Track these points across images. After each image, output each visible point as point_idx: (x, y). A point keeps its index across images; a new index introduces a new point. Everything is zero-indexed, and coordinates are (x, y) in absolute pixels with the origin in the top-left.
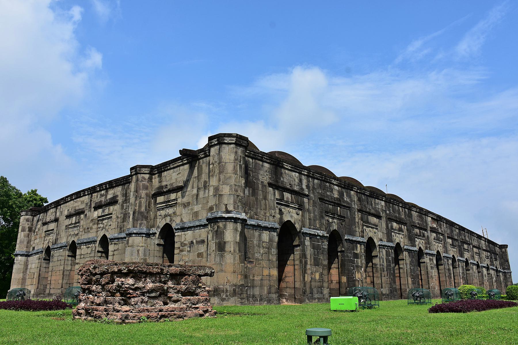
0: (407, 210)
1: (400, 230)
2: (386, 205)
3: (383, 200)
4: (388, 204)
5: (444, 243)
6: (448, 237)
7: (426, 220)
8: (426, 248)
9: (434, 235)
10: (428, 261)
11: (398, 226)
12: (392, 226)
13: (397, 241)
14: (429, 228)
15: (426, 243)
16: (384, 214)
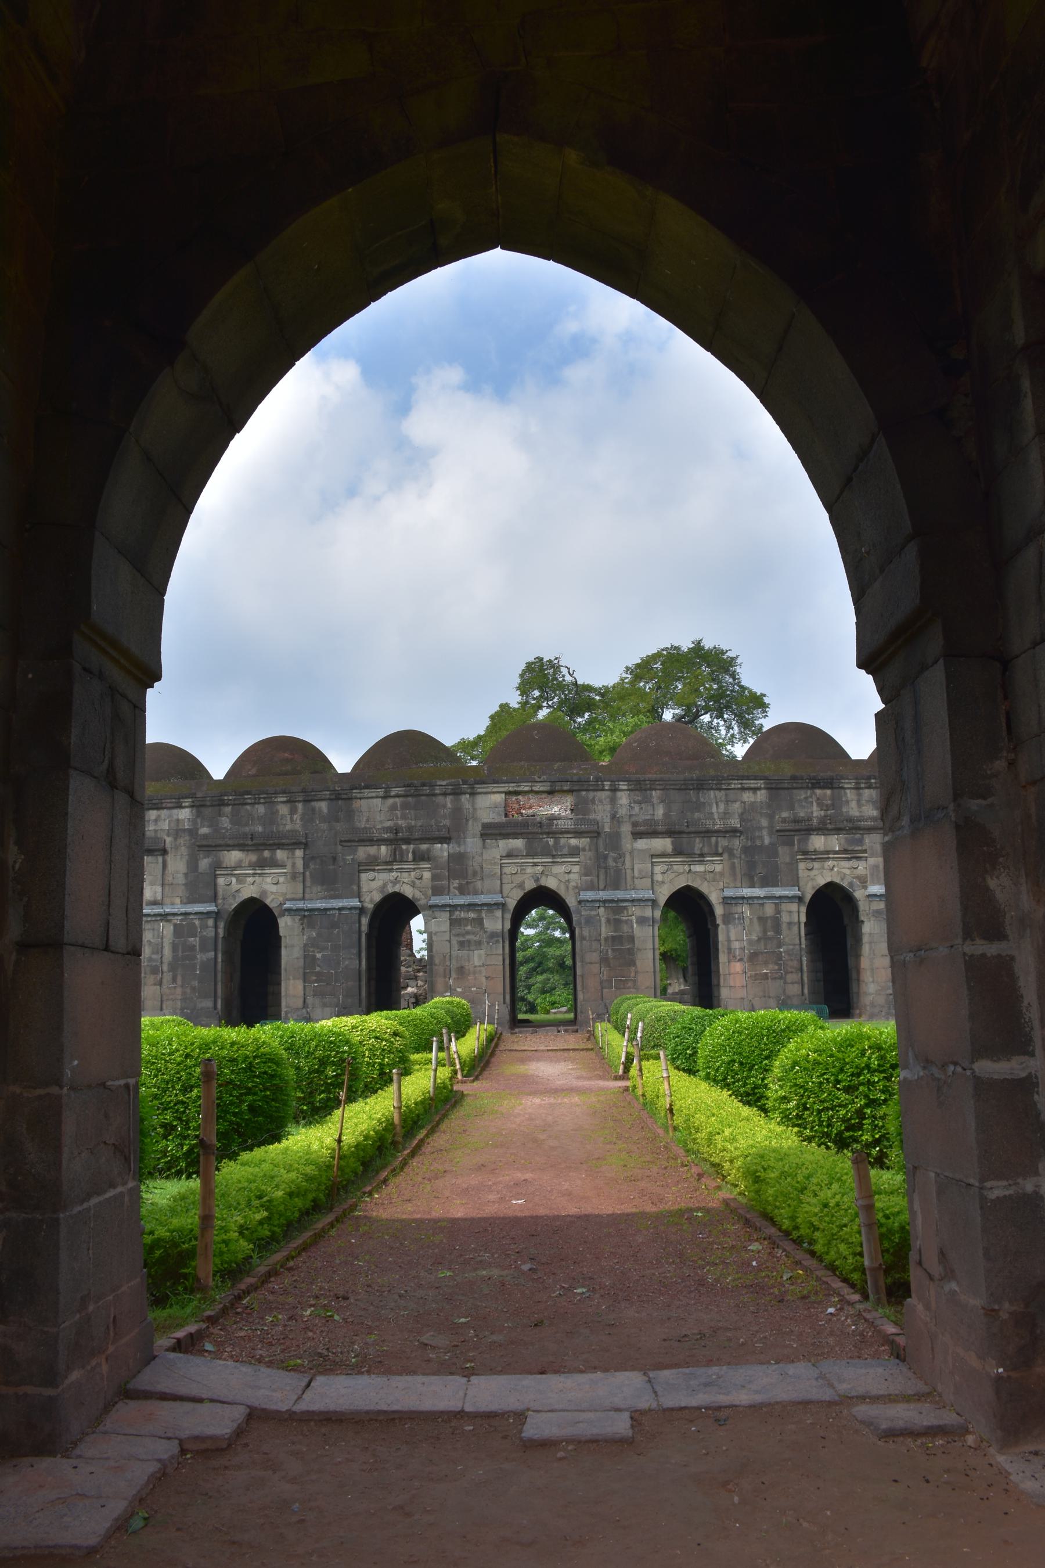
0: (323, 806)
1: (262, 864)
2: (199, 814)
3: (180, 807)
4: (207, 811)
5: (600, 860)
6: (637, 835)
7: (457, 811)
8: (437, 891)
9: (518, 843)
10: (446, 926)
11: (253, 857)
12: (217, 866)
13: (248, 891)
14: (474, 828)
15: (434, 878)
16: (184, 840)
